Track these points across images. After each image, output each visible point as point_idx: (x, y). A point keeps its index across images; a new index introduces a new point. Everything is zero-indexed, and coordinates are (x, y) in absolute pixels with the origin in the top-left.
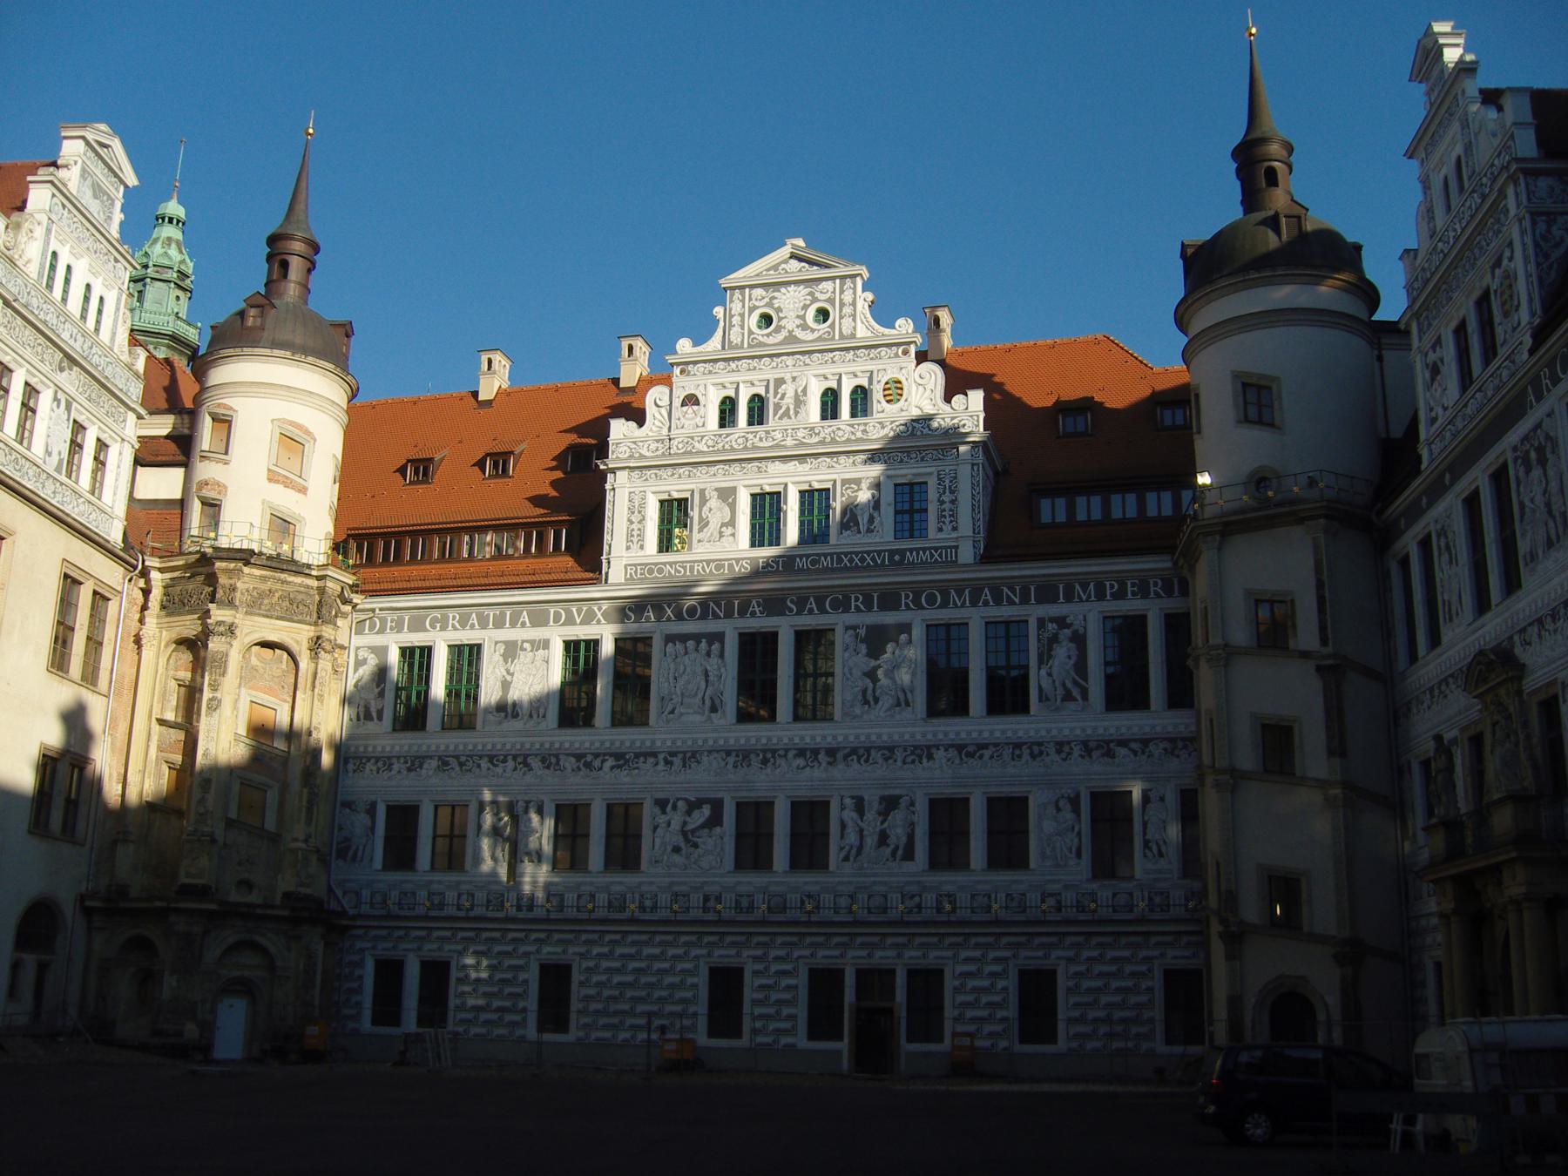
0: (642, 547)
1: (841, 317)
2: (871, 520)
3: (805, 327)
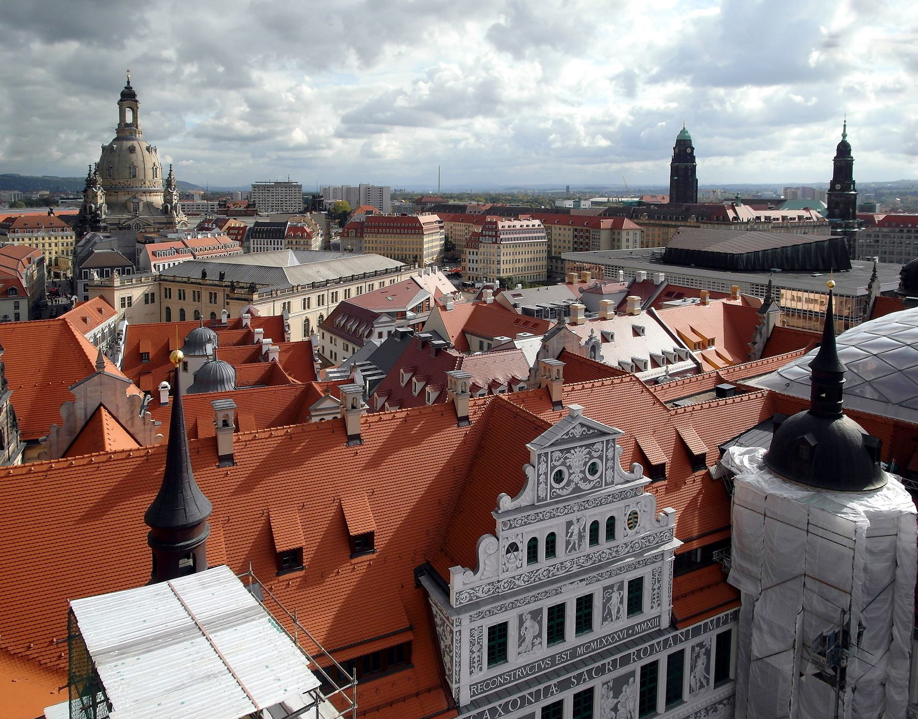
0: (481, 669)
1: (606, 470)
2: (618, 612)
3: (585, 479)
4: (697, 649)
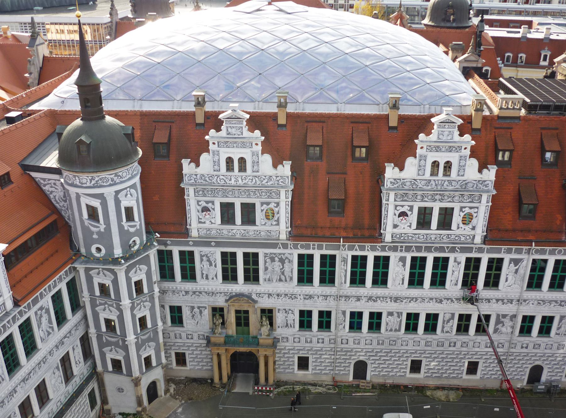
4: (39, 312)
